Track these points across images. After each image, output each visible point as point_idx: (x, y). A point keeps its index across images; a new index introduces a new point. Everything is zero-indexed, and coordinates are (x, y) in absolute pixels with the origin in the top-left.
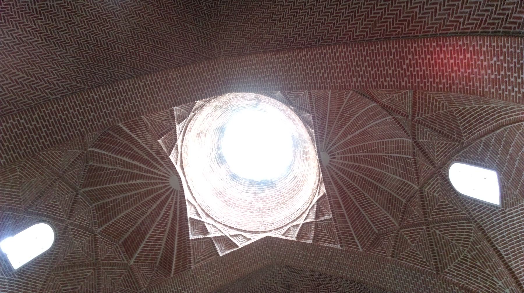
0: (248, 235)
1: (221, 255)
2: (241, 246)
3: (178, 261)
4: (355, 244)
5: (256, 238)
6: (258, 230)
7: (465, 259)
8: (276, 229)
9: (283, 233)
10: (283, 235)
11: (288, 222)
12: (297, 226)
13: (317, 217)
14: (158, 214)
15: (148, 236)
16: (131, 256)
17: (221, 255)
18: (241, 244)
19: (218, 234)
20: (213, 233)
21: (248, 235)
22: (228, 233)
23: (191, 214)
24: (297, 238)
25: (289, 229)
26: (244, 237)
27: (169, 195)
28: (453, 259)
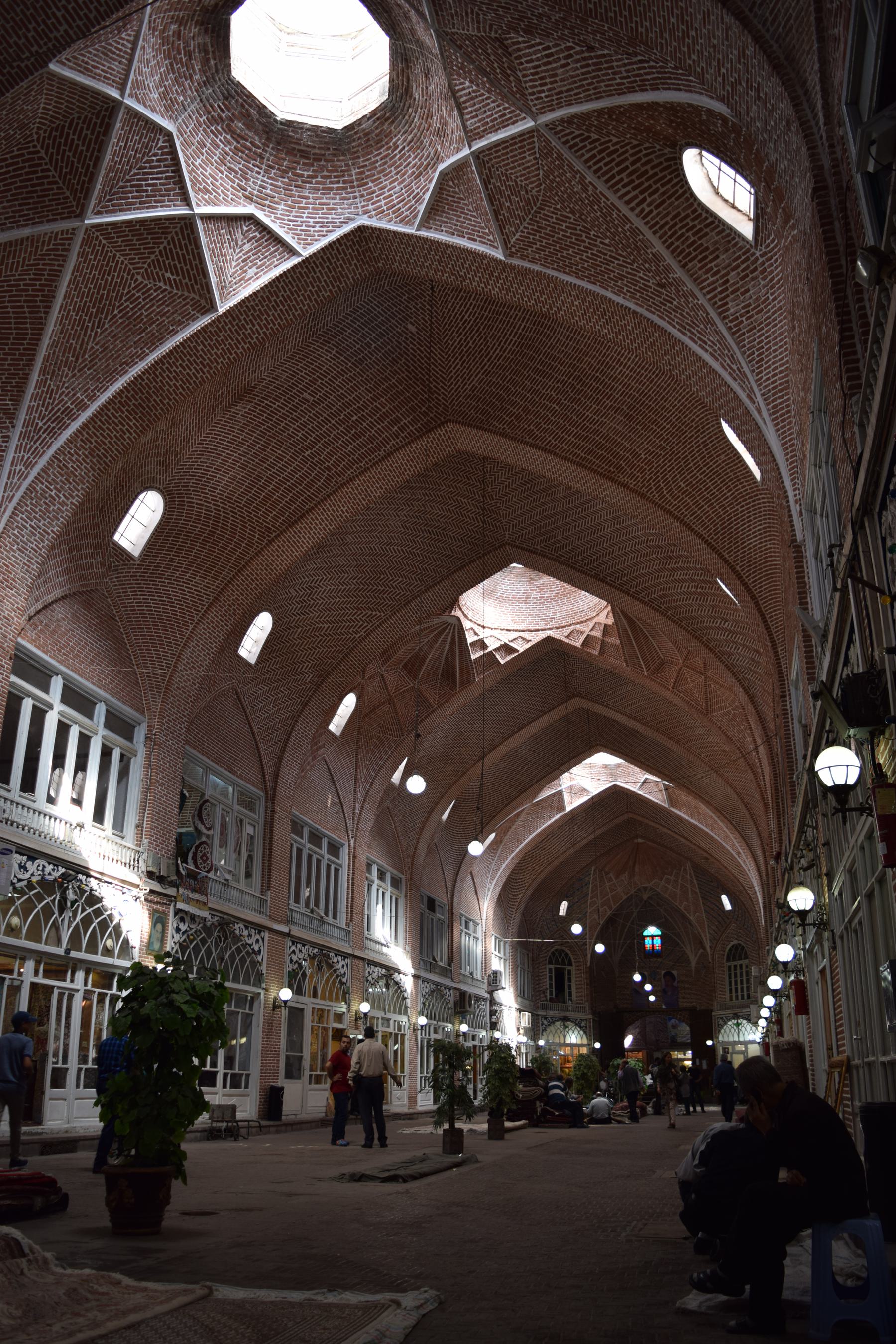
0: (527, 635)
2: (521, 650)
3: (461, 676)
4: (640, 666)
5: (536, 638)
6: (537, 627)
7: (729, 712)
8: (558, 628)
9: (566, 634)
10: (567, 637)
11: (571, 621)
12: (582, 633)
13: (604, 635)
14: (436, 642)
15: (428, 660)
16: (415, 677)
17: (502, 662)
18: (521, 647)
19: (497, 644)
20: (492, 645)
21: (527, 635)
22: (506, 638)
23: (470, 638)
24: (583, 644)
25: (572, 632)
26: (524, 639)
27: (447, 627)
28: (721, 708)
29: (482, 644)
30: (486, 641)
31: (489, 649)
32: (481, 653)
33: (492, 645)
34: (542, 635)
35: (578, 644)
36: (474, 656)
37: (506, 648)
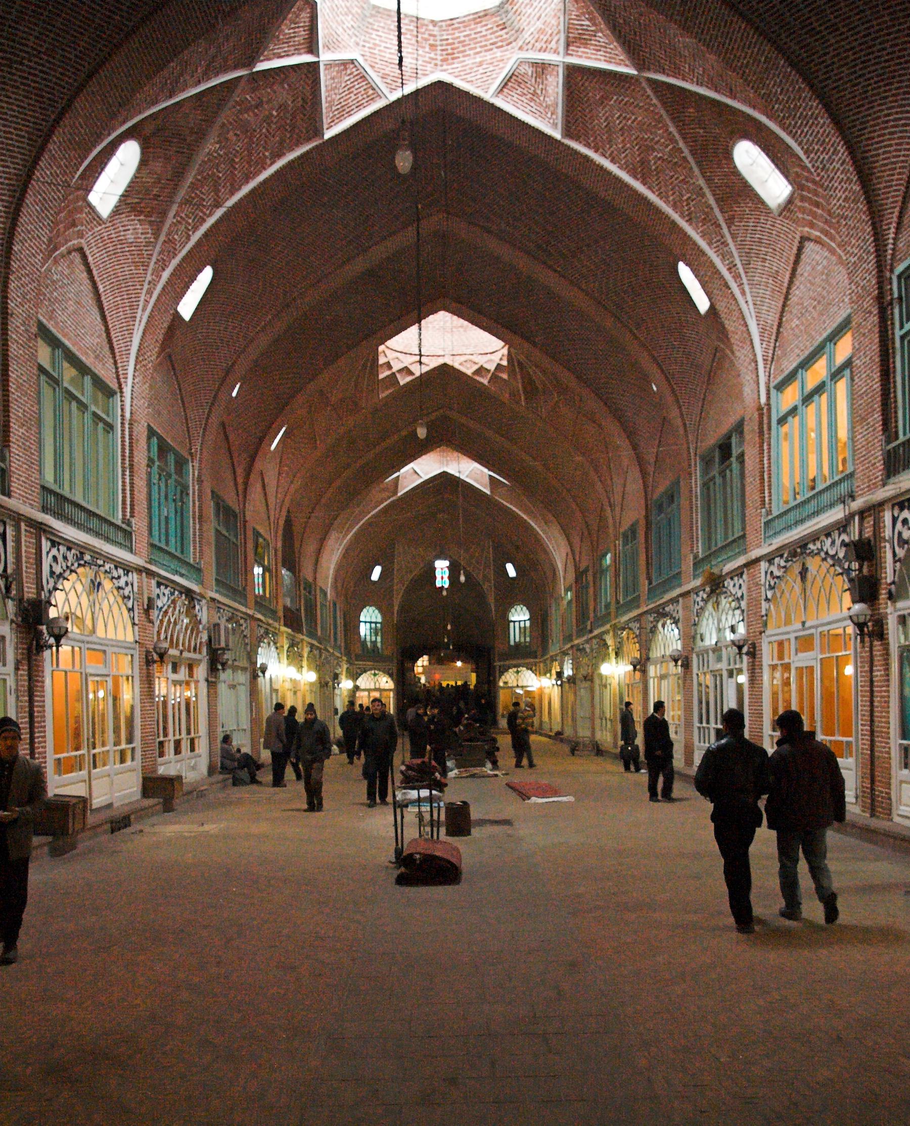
1: (402, 383)
5: (432, 363)
10: (461, 364)
17: (402, 383)
19: (401, 366)
20: (396, 366)
22: (407, 361)
23: (382, 360)
29: (388, 365)
30: (392, 363)
31: (395, 369)
32: (388, 373)
33: (396, 366)
34: (441, 361)
35: (469, 372)
36: (381, 376)
37: (406, 371)
